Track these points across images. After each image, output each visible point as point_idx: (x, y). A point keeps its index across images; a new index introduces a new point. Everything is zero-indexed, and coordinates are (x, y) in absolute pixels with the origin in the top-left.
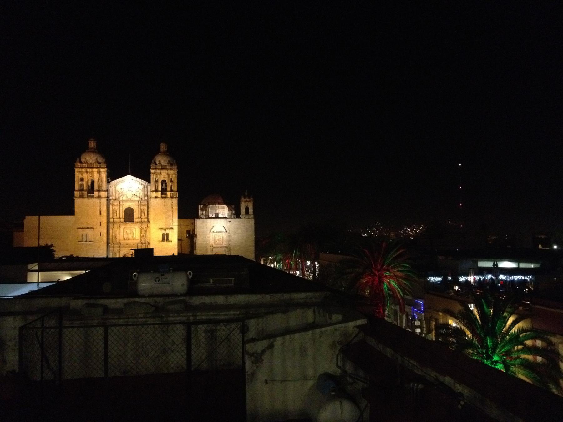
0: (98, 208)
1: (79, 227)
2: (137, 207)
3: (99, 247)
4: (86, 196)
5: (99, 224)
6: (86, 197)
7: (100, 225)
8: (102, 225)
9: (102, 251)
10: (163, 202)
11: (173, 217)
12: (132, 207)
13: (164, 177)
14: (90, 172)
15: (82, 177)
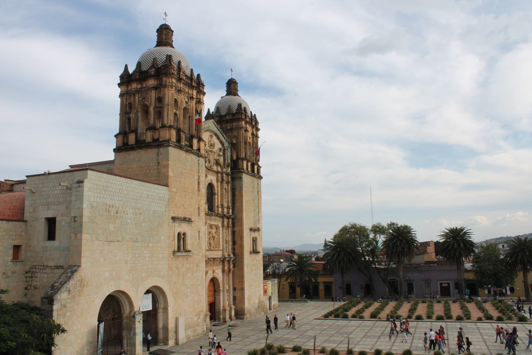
0: (197, 177)
1: (173, 215)
2: (219, 184)
3: (197, 266)
4: (184, 144)
5: (197, 212)
6: (183, 145)
7: (199, 215)
8: (201, 215)
9: (201, 273)
10: (252, 182)
11: (259, 210)
12: (214, 184)
13: (250, 138)
14: (186, 92)
15: (176, 98)
